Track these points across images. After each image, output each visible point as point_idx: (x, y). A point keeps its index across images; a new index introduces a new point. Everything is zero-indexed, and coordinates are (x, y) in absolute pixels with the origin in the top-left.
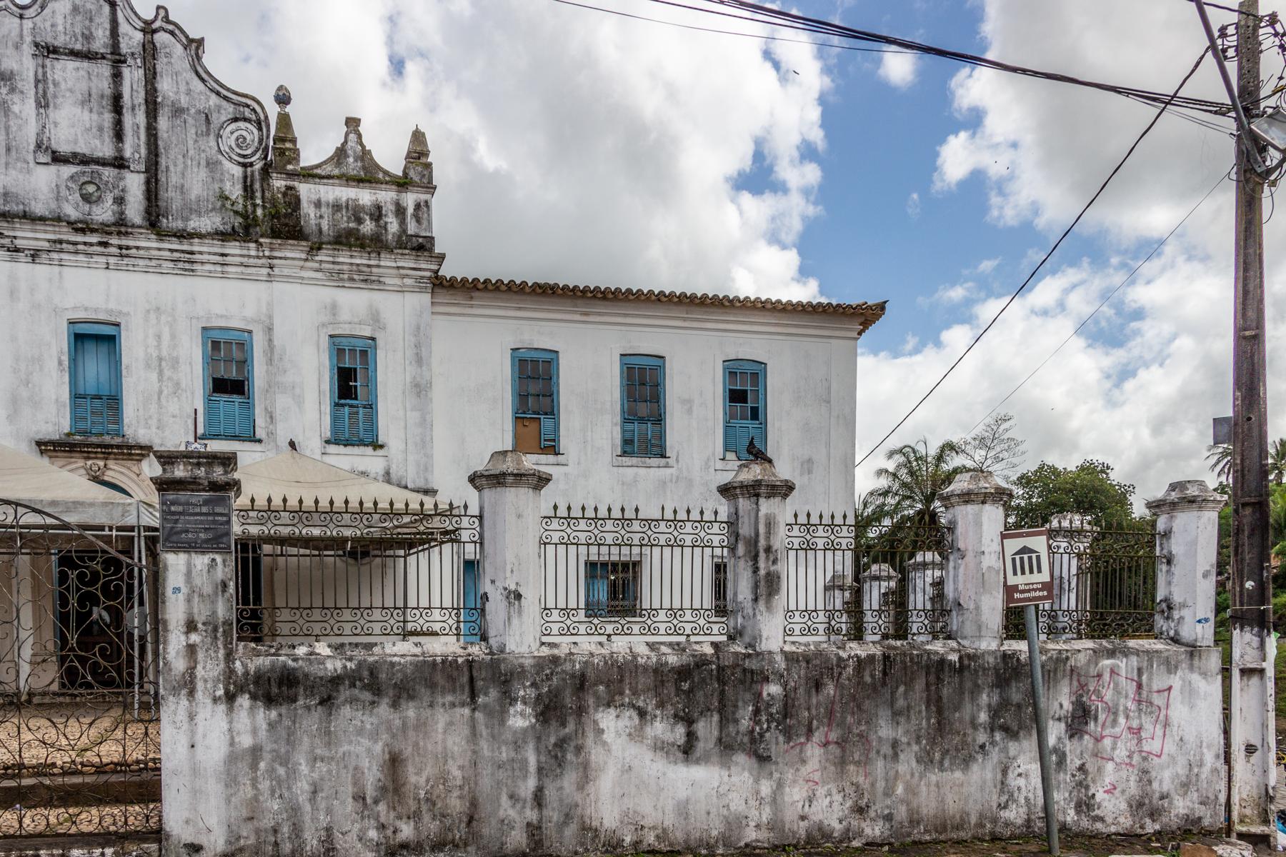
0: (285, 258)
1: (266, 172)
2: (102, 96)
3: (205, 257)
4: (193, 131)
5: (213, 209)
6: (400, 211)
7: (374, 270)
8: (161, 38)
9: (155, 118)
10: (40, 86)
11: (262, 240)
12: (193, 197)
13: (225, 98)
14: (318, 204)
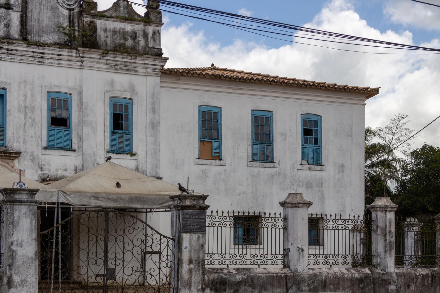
0: (90, 58)
1: (81, 13)
3: (50, 56)
5: (54, 31)
6: (145, 35)
7: (133, 65)
11: (79, 49)
12: (44, 25)
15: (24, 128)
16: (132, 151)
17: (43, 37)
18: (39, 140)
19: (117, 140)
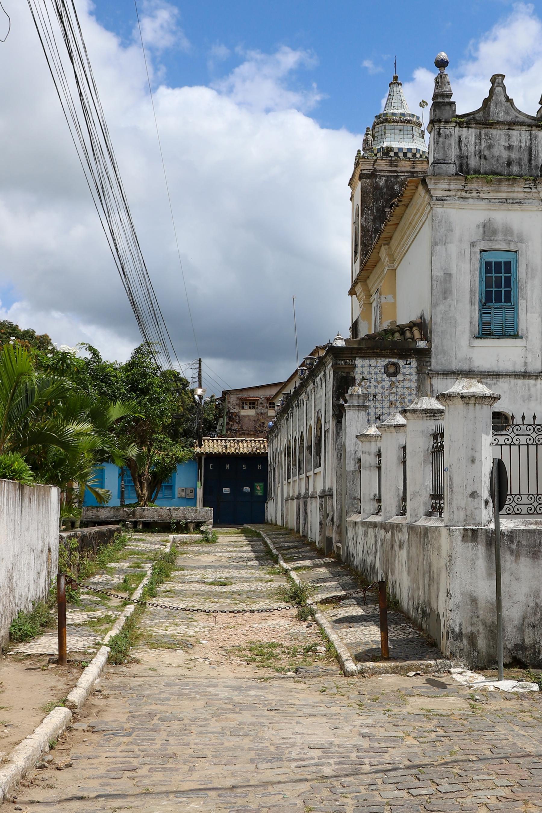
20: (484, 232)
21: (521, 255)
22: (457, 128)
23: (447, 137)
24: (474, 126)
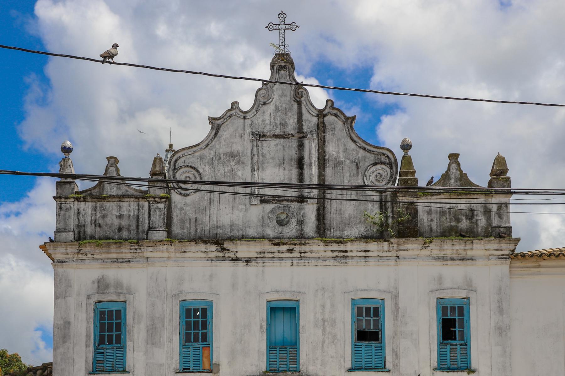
2: (291, 160)
4: (348, 175)
8: (329, 119)
9: (324, 169)
10: (255, 158)
13: (369, 151)
14: (430, 213)
15: (323, 346)
16: (470, 368)
17: (346, 232)
18: (342, 360)
19: (449, 354)
20: (99, 287)
21: (129, 305)
22: (76, 203)
23: (67, 210)
24: (90, 200)
